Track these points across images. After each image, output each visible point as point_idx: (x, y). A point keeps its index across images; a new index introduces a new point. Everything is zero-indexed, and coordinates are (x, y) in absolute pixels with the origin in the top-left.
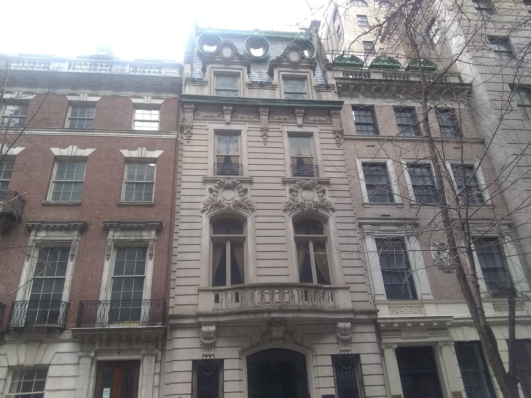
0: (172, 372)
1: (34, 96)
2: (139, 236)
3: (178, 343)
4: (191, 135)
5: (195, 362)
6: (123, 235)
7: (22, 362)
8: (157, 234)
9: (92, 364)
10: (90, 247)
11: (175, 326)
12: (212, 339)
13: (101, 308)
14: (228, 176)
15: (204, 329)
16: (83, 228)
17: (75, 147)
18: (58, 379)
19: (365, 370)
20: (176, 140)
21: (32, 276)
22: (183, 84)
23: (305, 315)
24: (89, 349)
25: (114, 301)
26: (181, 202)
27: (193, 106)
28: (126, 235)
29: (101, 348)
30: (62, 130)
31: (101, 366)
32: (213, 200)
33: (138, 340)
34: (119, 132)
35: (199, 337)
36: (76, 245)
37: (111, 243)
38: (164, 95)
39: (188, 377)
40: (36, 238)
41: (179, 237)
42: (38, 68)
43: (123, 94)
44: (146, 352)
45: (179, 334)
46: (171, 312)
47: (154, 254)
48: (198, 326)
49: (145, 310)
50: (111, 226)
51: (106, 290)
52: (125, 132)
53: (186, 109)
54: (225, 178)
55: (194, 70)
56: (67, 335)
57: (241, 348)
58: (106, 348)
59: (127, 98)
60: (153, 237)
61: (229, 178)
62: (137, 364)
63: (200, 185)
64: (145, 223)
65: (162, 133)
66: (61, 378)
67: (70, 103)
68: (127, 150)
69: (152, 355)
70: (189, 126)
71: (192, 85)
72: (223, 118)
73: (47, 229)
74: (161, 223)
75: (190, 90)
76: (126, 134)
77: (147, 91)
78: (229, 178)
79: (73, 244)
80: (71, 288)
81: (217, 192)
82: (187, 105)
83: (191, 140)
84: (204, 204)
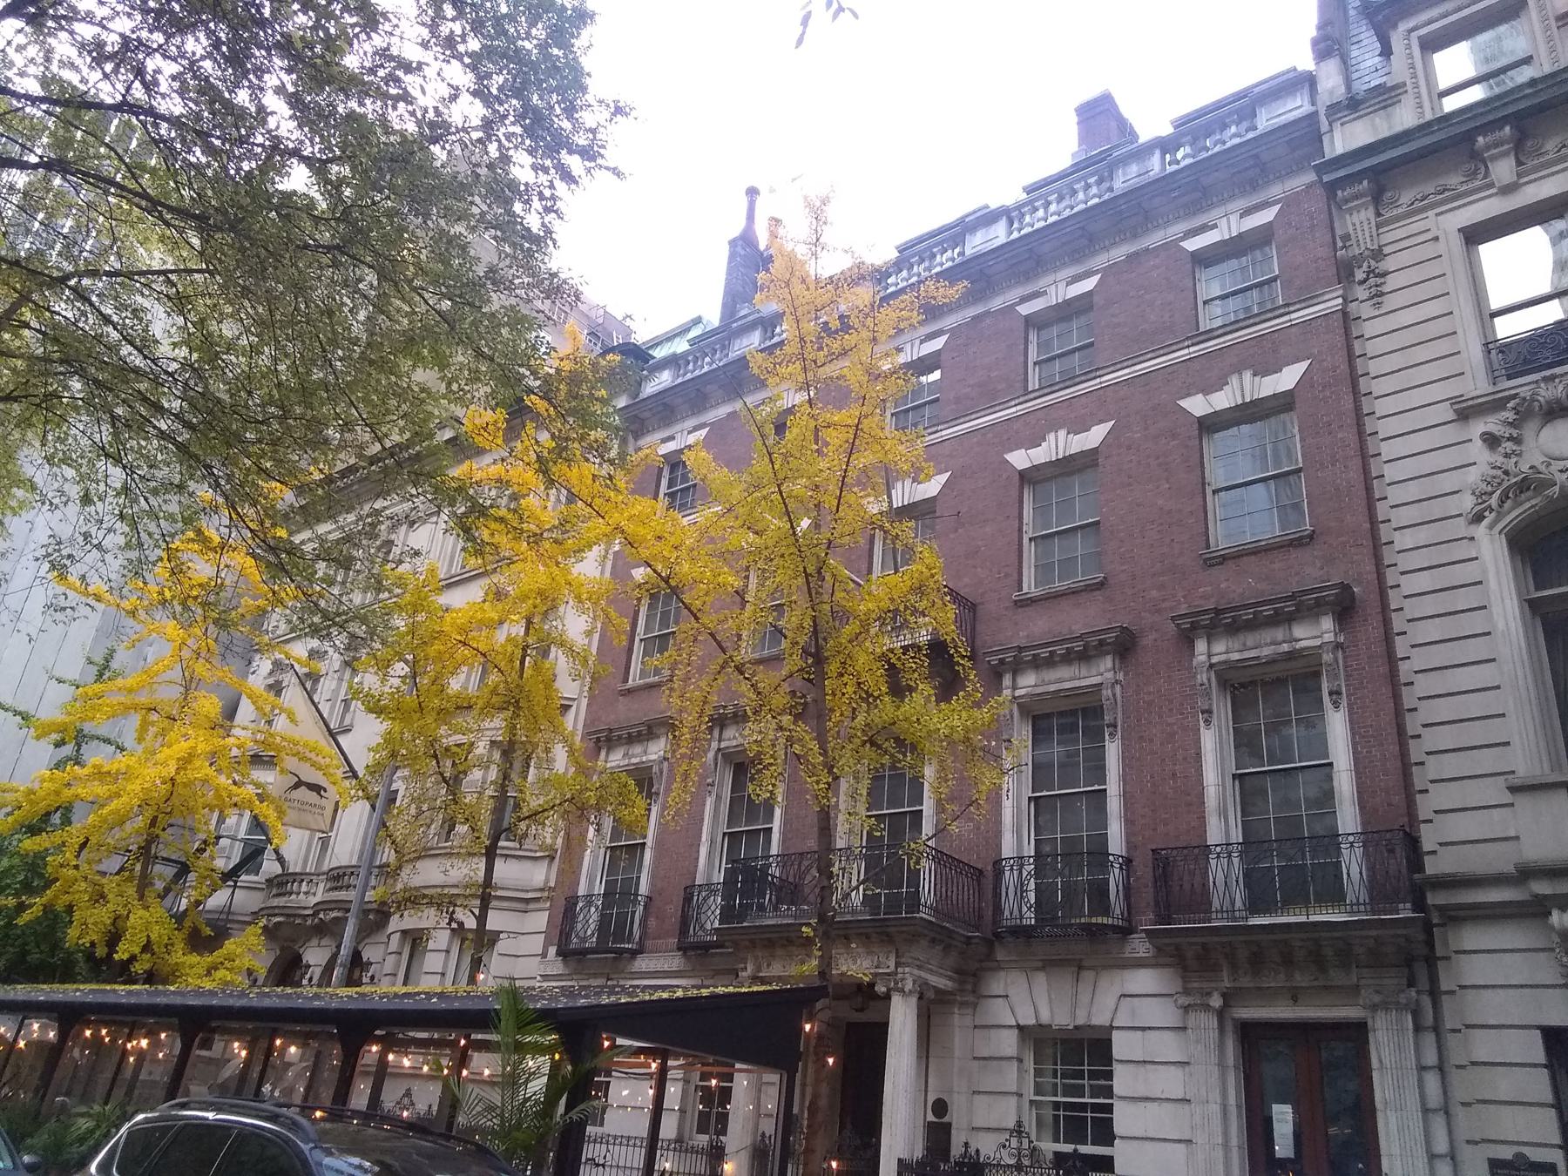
0: (1474, 1064)
2: (1284, 642)
3: (1475, 970)
4: (1382, 280)
6: (1237, 646)
7: (1045, 1017)
8: (1340, 625)
10: (1151, 697)
11: (1453, 913)
13: (1217, 869)
14: (1548, 373)
16: (1124, 646)
17: (1062, 433)
18: (1141, 1069)
20: (1344, 313)
22: (1324, 127)
24: (1205, 985)
25: (1252, 844)
26: (1392, 507)
27: (1365, 183)
28: (1244, 645)
29: (1237, 985)
30: (1021, 399)
31: (1252, 1038)
32: (1506, 473)
33: (1346, 958)
34: (1166, 350)
35: (1552, 950)
36: (1114, 695)
37: (1205, 676)
38: (1276, 191)
39: (1539, 1085)
40: (1018, 693)
41: (1409, 621)
42: (942, 264)
43: (1155, 239)
44: (1377, 999)
45: (1472, 937)
46: (1432, 867)
47: (1344, 689)
48: (1537, 910)
49: (1353, 864)
50: (1194, 627)
51: (1223, 813)
52: (1181, 346)
53: (1347, 201)
54: (1537, 382)
55: (1354, 69)
56: (1140, 947)
58: (1251, 985)
59: (1172, 246)
60: (1329, 637)
61: (1552, 378)
62: (1358, 1032)
63: (1451, 433)
64: (1293, 597)
65: (1292, 309)
66: (1149, 1067)
67: (1029, 321)
68: (1200, 396)
69: (1400, 1008)
70: (1366, 253)
71: (1355, 119)
72: (1485, 177)
73: (1037, 664)
74: (1345, 588)
75: (1345, 139)
76: (1186, 351)
77: (1223, 202)
78: (1552, 378)
79: (1106, 693)
80: (1125, 815)
81: (1517, 440)
82: (1343, 190)
83: (1383, 294)
84: (1473, 493)
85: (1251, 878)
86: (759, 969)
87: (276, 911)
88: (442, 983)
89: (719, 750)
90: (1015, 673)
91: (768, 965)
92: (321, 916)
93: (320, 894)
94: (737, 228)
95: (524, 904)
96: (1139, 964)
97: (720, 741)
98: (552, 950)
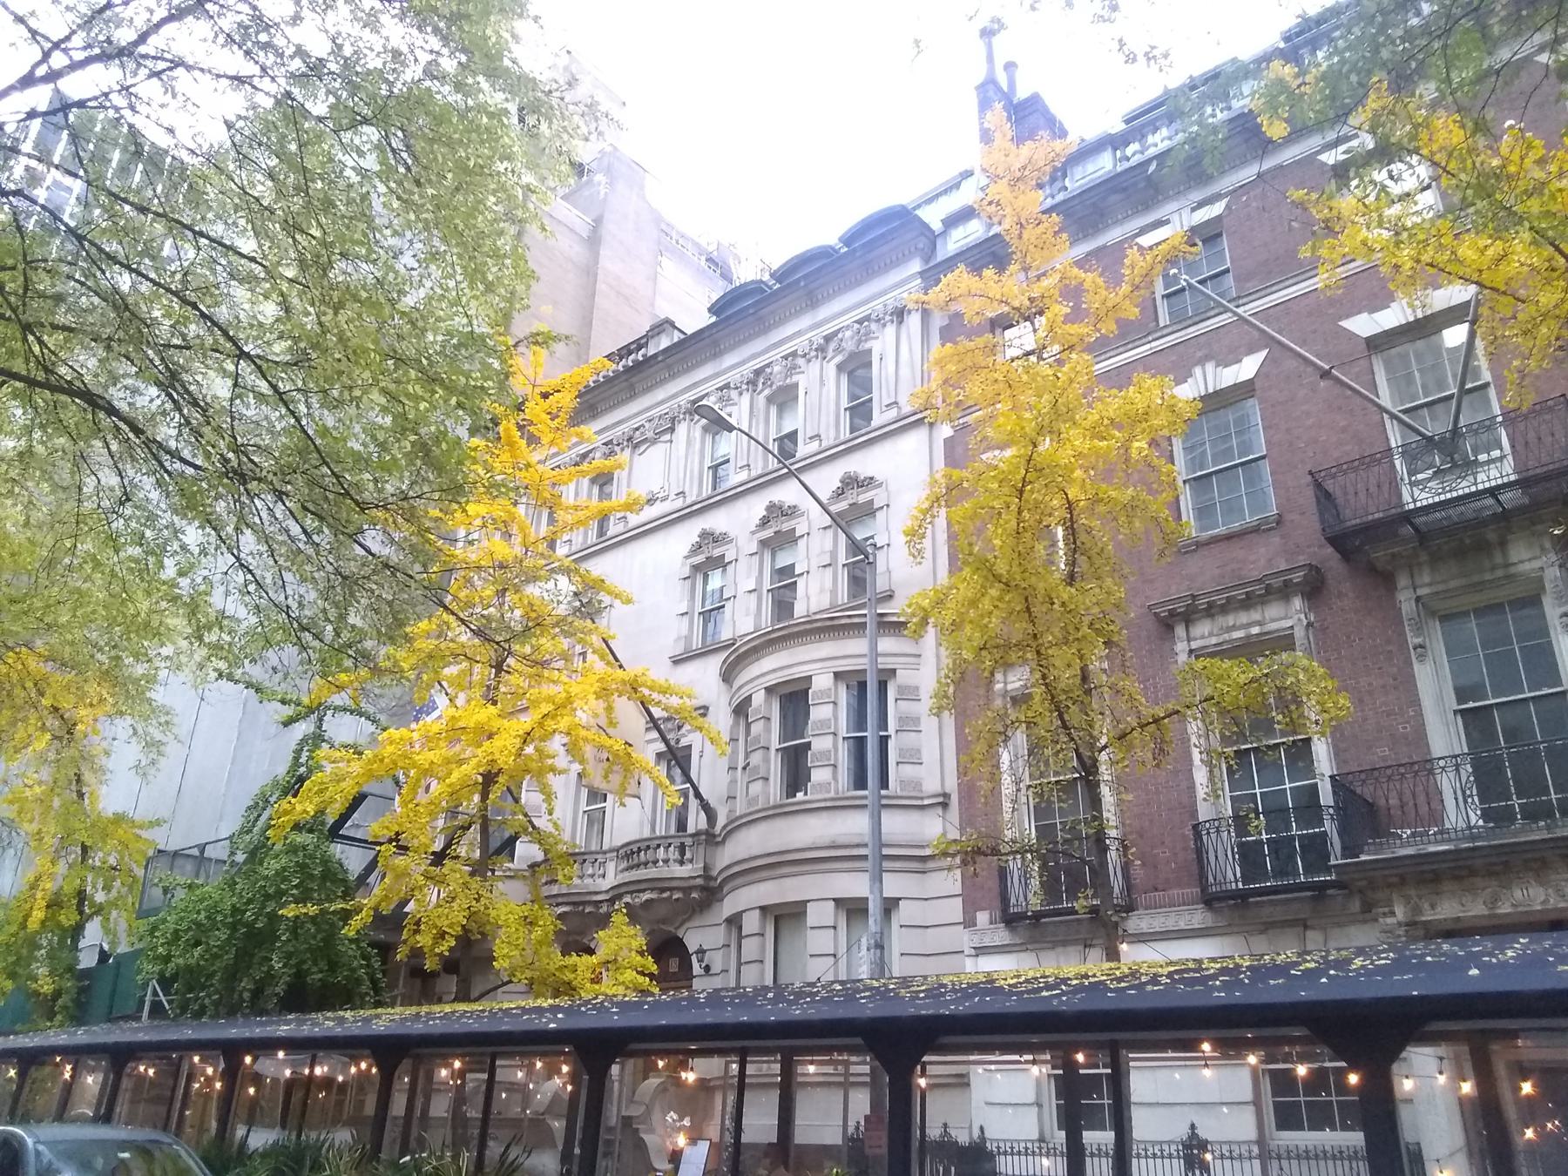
1: (1226, 200)
86: (1417, 910)
87: (560, 900)
91: (1433, 907)
92: (627, 899)
93: (611, 876)
94: (980, 77)
95: (919, 862)
98: (982, 918)
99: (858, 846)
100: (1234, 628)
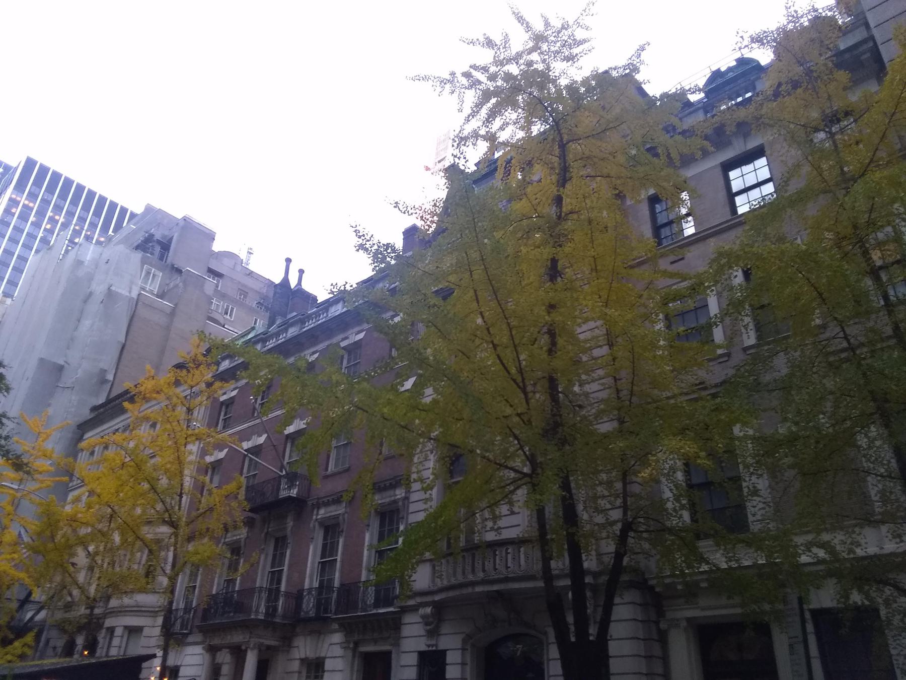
5: (422, 654)
9: (354, 656)
12: (432, 623)
15: (422, 611)
19: (615, 665)
21: (318, 559)
23: (516, 586)
40: (319, 517)
45: (408, 618)
48: (414, 609)
57: (463, 636)
60: (403, 495)
73: (327, 504)
79: (341, 518)
85: (377, 592)
88: (119, 651)
89: (224, 543)
90: (319, 508)
95: (153, 614)
96: (335, 631)
97: (225, 538)
99: (134, 607)
100: (234, 536)
